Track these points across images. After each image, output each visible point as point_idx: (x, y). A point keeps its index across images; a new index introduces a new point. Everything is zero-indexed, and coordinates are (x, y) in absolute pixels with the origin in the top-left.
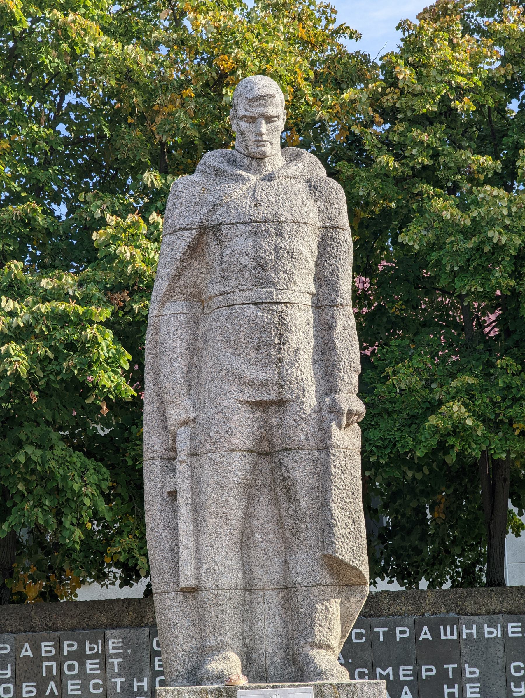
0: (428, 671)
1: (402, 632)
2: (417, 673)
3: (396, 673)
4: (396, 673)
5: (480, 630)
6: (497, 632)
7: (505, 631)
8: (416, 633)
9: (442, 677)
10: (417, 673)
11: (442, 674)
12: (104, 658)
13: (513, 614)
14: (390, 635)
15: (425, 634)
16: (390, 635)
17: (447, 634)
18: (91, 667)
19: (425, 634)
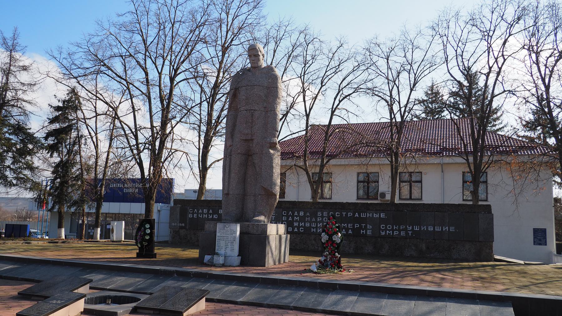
0: (357, 226)
1: (350, 214)
2: (353, 226)
3: (348, 226)
4: (348, 226)
5: (373, 215)
6: (378, 216)
7: (380, 215)
8: (354, 214)
9: (361, 228)
10: (353, 226)
11: (361, 227)
13: (383, 211)
14: (346, 215)
15: (357, 215)
16: (346, 215)
17: (363, 215)
19: (357, 215)
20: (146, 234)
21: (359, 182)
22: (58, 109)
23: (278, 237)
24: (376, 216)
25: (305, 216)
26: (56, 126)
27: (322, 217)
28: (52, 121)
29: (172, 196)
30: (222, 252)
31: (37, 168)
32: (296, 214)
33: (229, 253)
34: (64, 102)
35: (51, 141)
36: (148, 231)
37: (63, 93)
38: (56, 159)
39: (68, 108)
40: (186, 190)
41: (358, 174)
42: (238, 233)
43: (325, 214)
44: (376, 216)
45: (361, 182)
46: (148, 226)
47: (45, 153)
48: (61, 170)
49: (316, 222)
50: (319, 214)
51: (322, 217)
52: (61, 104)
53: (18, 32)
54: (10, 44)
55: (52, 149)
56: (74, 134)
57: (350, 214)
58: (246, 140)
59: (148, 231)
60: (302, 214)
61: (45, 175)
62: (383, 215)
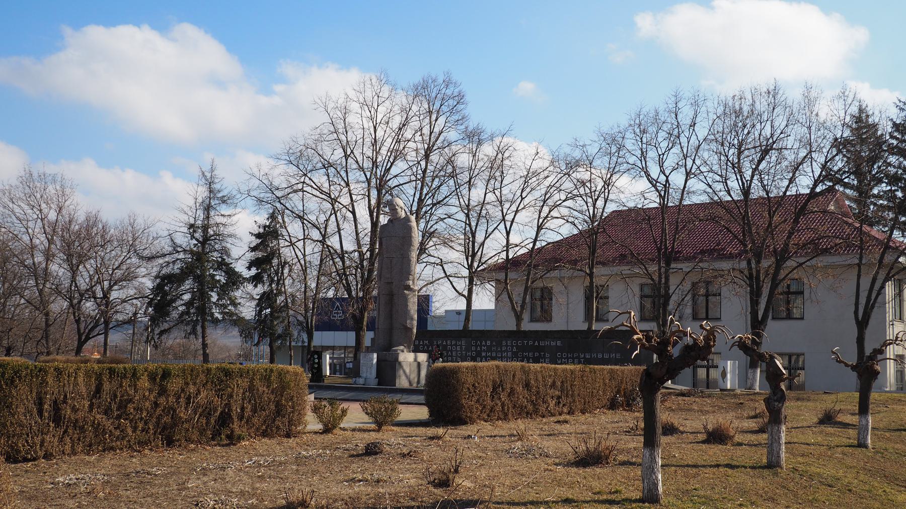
1: (531, 343)
12: (461, 345)
15: (536, 344)
18: (458, 348)
19: (536, 344)
20: (314, 363)
21: (642, 297)
22: (258, 236)
23: (416, 364)
24: (553, 344)
25: (491, 345)
26: (260, 254)
27: (507, 346)
28: (253, 249)
29: (429, 320)
30: (364, 375)
31: (239, 304)
32: (484, 343)
33: (369, 376)
34: (265, 227)
35: (254, 271)
36: (317, 361)
37: (263, 219)
38: (260, 289)
39: (267, 236)
40: (446, 311)
41: (642, 286)
42: (375, 361)
43: (509, 343)
44: (553, 344)
45: (647, 297)
46: (316, 356)
47: (250, 287)
48: (266, 300)
49: (501, 351)
50: (504, 343)
51: (507, 346)
52: (262, 230)
53: (215, 163)
54: (208, 175)
55: (256, 280)
56: (275, 261)
57: (531, 343)
58: (388, 283)
59: (317, 361)
60: (489, 343)
61: (248, 311)
62: (559, 343)
